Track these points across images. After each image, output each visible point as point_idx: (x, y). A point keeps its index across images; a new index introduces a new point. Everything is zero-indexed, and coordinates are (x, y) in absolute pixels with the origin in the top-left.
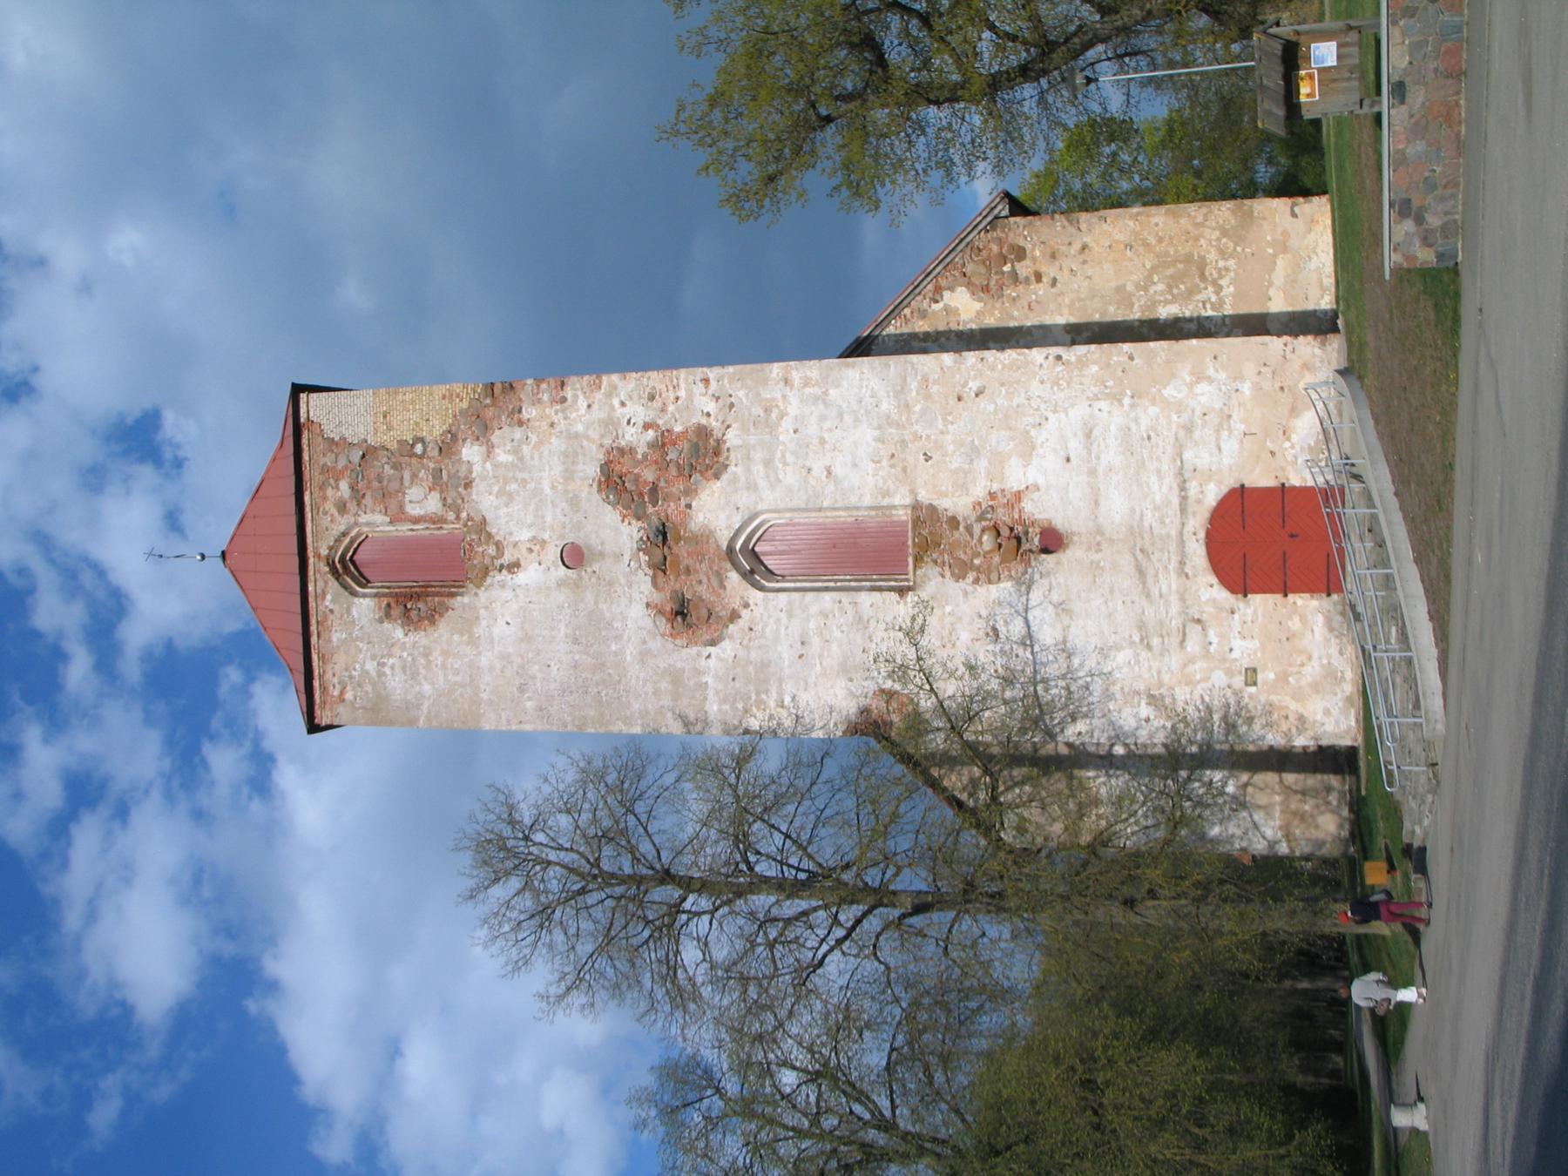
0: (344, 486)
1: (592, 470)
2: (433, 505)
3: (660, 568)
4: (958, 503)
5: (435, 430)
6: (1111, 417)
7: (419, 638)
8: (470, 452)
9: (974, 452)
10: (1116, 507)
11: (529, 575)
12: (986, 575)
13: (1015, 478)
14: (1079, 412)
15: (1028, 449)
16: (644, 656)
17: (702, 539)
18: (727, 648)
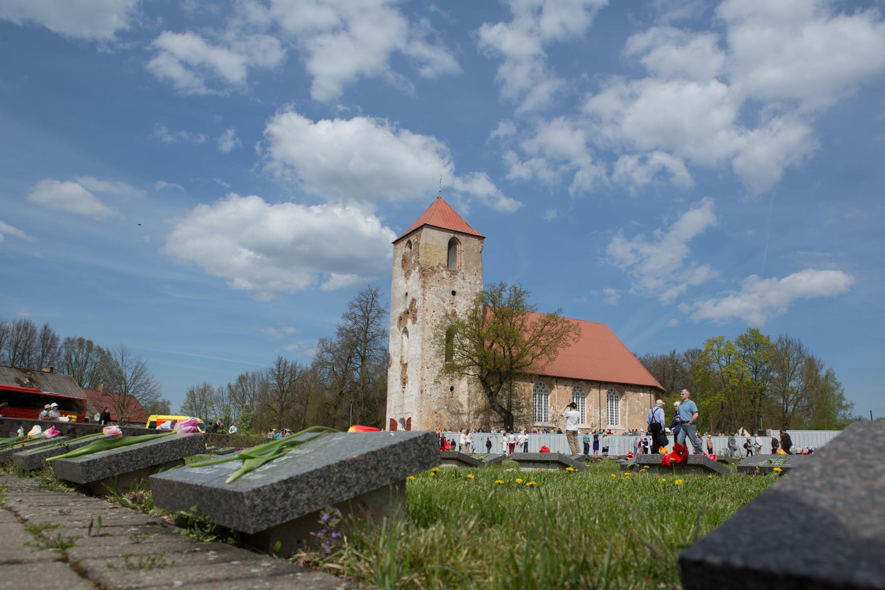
0: (416, 240)
1: (415, 297)
2: (413, 262)
3: (404, 313)
4: (407, 372)
5: (420, 260)
6: (413, 400)
7: (400, 265)
8: (417, 268)
9: (412, 374)
10: (406, 401)
11: (405, 286)
12: (402, 377)
13: (410, 382)
14: (415, 394)
15: (412, 384)
16: (397, 312)
17: (406, 322)
18: (397, 329)
